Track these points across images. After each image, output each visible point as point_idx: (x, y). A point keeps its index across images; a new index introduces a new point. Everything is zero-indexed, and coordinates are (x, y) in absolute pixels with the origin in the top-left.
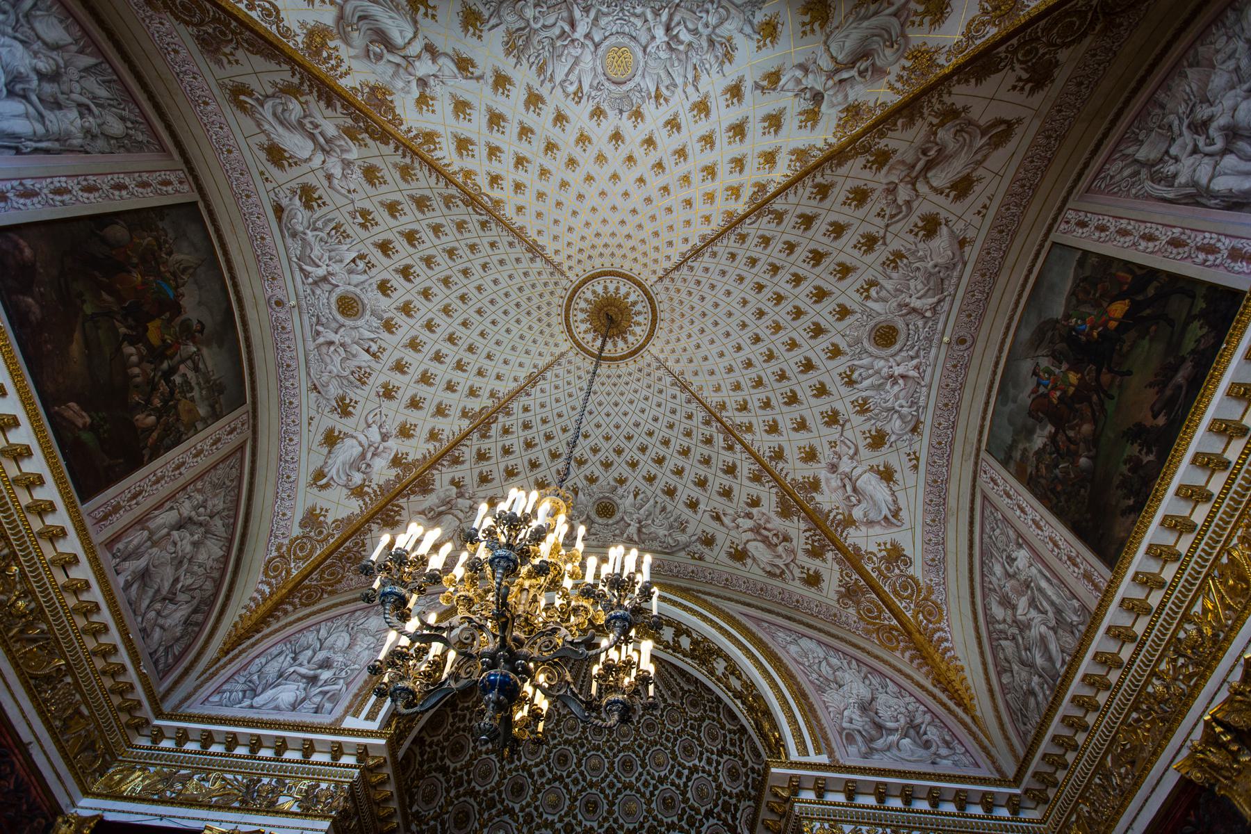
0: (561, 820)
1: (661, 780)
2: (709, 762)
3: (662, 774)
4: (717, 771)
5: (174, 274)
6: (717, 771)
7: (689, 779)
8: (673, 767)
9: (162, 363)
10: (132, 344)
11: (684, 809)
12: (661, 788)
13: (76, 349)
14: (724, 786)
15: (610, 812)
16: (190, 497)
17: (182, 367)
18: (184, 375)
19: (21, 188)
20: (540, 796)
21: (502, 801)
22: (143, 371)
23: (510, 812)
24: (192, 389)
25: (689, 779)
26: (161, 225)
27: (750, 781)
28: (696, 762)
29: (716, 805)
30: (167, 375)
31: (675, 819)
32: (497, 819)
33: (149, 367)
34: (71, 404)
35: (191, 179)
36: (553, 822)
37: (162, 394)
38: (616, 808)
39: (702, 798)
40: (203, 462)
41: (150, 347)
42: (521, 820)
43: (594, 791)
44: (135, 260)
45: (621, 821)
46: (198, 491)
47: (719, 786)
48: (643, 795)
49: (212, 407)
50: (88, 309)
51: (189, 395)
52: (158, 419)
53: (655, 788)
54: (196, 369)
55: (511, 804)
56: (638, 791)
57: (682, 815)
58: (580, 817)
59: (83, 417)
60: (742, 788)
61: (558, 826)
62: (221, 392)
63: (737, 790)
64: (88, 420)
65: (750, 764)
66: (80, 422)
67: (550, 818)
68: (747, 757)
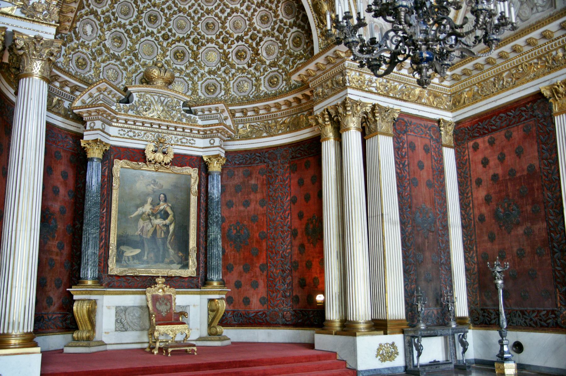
0: (131, 24)
1: (208, 12)
2: (248, 8)
3: (210, 8)
4: (253, 14)
6: (253, 14)
7: (229, 15)
8: (219, 5)
11: (221, 32)
12: (207, 16)
14: (256, 25)
15: (166, 25)
20: (116, 5)
21: (89, 6)
23: (95, 13)
25: (229, 15)
27: (277, 27)
28: (238, 6)
29: (246, 35)
31: (214, 37)
32: (85, 17)
36: (125, 24)
38: (171, 22)
39: (236, 28)
42: (102, 20)
43: (156, 9)
45: (174, 31)
47: (251, 25)
48: (192, 18)
53: (202, 15)
55: (95, 8)
56: (189, 15)
57: (220, 35)
58: (144, 24)
60: (269, 29)
61: (129, 27)
63: (265, 30)
65: (281, 17)
67: (123, 21)
68: (279, 12)
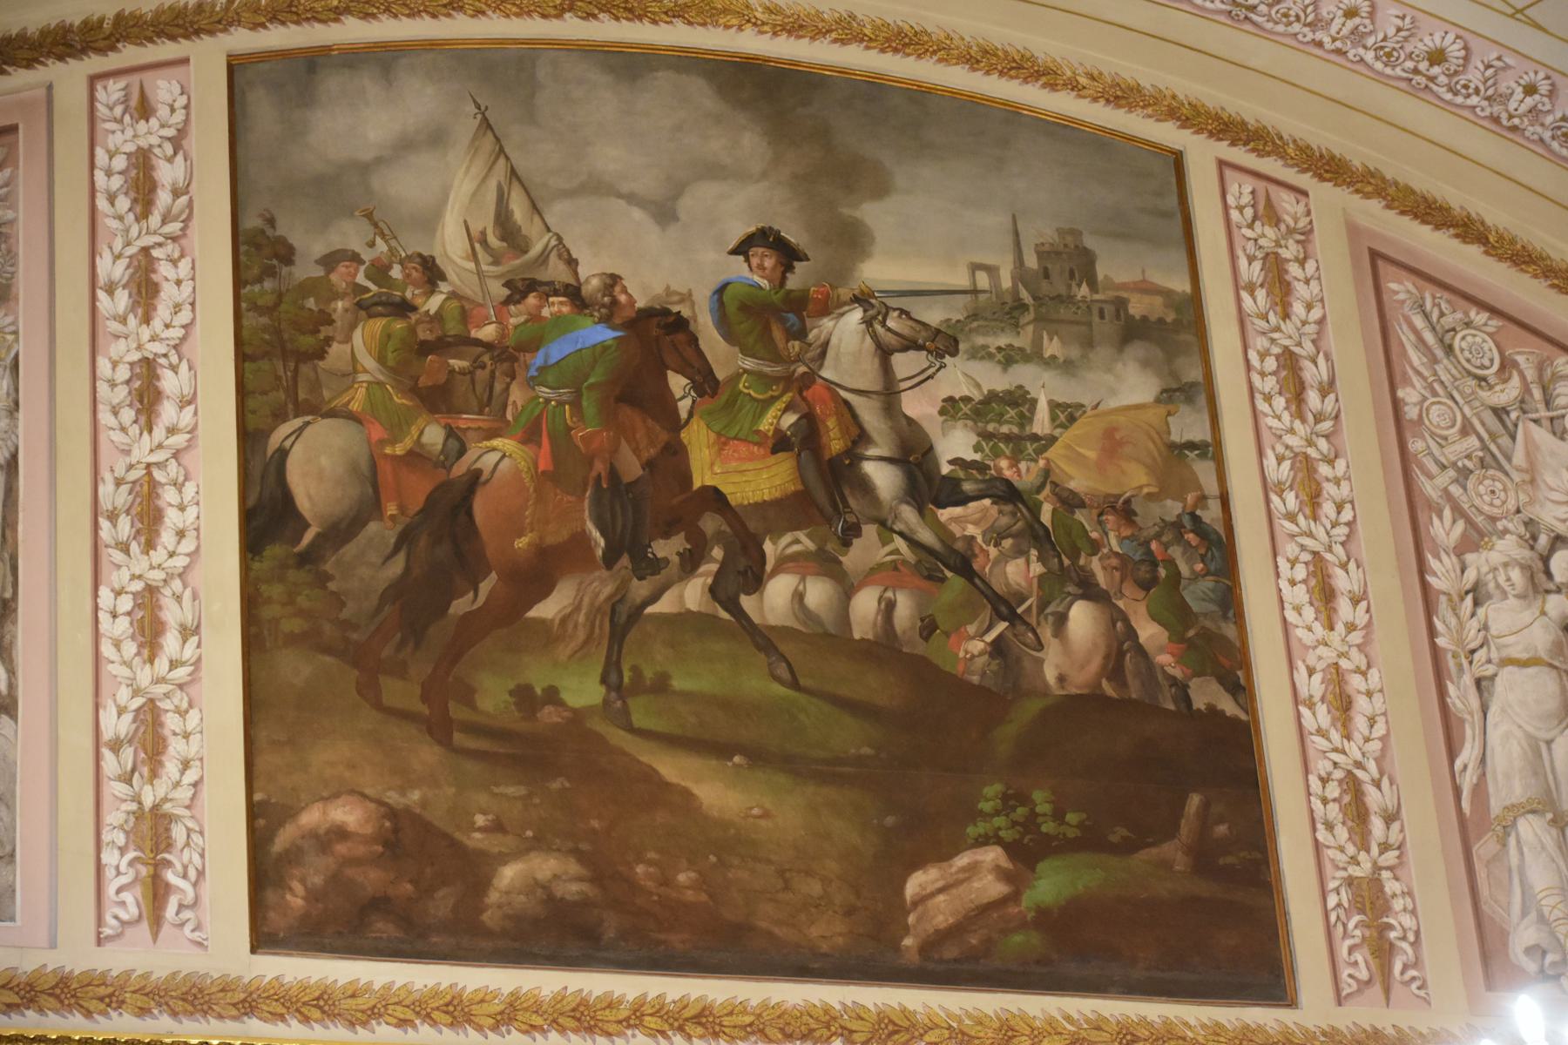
5: (520, 289)
9: (865, 487)
10: (755, 580)
13: (718, 792)
16: (1478, 595)
17: (916, 405)
18: (951, 407)
19: (128, 754)
22: (872, 574)
24: (1019, 400)
26: (305, 270)
30: (928, 485)
33: (867, 550)
34: (915, 884)
35: (130, 54)
37: (996, 536)
40: (1359, 474)
41: (792, 510)
44: (434, 435)
46: (1474, 539)
49: (1132, 331)
50: (583, 690)
51: (1042, 423)
52: (1089, 590)
54: (942, 343)
59: (973, 869)
62: (1083, 266)
64: (992, 855)
66: (990, 887)
